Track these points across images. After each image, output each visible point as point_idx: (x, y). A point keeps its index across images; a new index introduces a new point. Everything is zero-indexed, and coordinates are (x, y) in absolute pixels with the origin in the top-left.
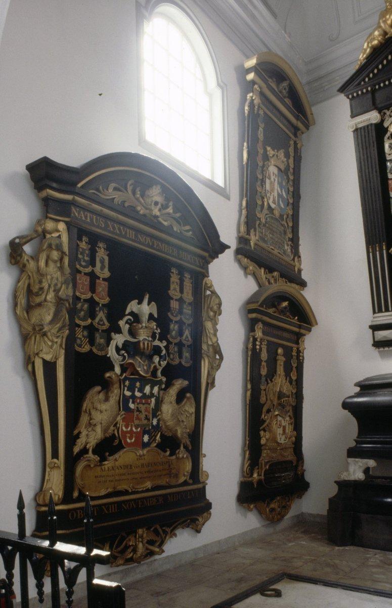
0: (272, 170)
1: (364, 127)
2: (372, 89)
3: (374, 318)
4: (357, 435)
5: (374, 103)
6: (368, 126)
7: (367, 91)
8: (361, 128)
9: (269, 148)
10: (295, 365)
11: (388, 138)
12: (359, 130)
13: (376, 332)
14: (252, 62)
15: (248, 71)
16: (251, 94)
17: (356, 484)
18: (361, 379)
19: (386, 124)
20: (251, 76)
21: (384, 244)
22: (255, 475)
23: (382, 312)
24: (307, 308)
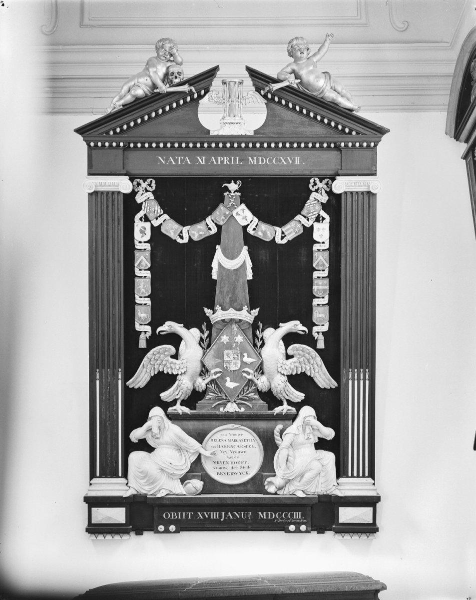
1: (108, 192)
2: (124, 146)
3: (91, 484)
6: (113, 193)
7: (118, 146)
8: (102, 193)
11: (141, 219)
12: (99, 195)
13: (93, 509)
19: (139, 199)
21: (120, 370)
23: (118, 477)
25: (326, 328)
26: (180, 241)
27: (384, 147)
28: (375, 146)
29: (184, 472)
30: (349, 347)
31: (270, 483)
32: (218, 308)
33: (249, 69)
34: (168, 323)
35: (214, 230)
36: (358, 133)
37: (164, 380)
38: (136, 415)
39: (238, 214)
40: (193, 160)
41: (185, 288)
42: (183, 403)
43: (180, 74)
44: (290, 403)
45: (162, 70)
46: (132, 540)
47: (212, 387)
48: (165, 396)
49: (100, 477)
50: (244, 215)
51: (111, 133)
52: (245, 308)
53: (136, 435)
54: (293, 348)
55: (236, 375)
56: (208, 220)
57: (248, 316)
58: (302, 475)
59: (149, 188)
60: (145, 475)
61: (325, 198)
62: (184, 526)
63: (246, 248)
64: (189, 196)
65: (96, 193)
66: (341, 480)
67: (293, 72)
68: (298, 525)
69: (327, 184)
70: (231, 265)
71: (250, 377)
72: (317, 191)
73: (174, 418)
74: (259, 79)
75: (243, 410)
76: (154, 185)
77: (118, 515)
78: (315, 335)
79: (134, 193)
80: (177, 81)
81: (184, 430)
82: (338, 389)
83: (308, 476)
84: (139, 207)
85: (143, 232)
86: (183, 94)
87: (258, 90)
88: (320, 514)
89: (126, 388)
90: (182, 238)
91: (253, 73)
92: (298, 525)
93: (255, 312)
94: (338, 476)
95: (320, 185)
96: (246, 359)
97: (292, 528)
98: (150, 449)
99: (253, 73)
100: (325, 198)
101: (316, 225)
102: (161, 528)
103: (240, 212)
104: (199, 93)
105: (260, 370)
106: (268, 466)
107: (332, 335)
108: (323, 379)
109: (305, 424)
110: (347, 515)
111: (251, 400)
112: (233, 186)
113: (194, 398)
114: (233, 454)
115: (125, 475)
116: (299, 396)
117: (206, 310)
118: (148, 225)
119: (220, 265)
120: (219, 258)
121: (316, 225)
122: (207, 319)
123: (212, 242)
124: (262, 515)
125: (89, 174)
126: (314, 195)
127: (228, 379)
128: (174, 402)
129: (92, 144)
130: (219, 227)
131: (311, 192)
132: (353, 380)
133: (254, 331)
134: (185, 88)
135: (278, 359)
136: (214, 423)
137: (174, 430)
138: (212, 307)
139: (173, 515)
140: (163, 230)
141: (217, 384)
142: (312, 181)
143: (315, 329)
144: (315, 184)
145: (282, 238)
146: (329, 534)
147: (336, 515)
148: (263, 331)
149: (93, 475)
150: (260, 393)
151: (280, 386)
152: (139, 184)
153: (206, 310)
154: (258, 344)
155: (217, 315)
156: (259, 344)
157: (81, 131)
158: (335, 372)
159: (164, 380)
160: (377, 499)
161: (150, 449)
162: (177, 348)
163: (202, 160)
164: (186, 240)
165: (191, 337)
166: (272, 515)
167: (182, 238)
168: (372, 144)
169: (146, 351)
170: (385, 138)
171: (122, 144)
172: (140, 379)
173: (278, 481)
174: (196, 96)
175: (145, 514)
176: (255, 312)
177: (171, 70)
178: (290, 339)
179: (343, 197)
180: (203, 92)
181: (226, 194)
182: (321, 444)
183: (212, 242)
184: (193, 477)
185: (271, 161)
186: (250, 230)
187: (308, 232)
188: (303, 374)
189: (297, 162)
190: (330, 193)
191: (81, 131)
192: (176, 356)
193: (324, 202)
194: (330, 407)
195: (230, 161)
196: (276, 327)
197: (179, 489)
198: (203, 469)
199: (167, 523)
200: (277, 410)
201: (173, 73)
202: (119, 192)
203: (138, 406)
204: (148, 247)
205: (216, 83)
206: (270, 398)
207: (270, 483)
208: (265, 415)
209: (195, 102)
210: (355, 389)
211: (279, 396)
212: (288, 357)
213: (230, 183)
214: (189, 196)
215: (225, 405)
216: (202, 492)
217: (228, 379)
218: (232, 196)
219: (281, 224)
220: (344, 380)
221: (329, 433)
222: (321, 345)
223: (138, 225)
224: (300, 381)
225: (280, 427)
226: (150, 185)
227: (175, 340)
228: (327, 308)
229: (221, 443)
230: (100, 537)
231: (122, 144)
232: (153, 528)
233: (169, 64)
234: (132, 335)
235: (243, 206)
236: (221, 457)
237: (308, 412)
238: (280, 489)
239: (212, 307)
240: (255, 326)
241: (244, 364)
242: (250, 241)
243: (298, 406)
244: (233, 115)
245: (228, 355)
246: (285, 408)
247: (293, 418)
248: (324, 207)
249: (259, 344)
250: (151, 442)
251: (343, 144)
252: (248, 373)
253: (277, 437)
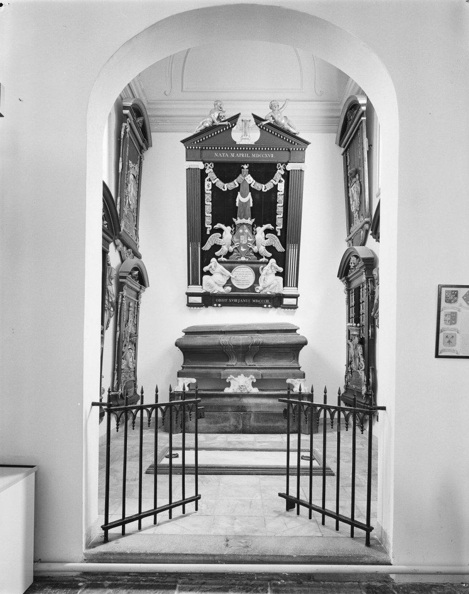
0: (131, 177)
1: (194, 169)
4: (182, 362)
5: (201, 157)
6: (196, 169)
7: (198, 148)
8: (192, 169)
9: (130, 162)
10: (136, 314)
13: (189, 297)
14: (129, 104)
15: (126, 108)
16: (126, 124)
17: (184, 395)
18: (186, 328)
19: (207, 171)
20: (126, 112)
22: (120, 390)
24: (145, 277)
25: (281, 227)
26: (223, 190)
27: (309, 150)
28: (305, 150)
29: (224, 284)
30: (290, 235)
31: (258, 289)
32: (238, 218)
33: (253, 115)
34: (218, 224)
35: (237, 185)
36: (298, 144)
37: (217, 247)
38: (206, 262)
39: (247, 179)
40: (230, 155)
41: (225, 209)
42: (224, 257)
43: (224, 116)
44: (266, 257)
45: (216, 115)
46: (204, 309)
47: (235, 250)
48: (217, 253)
49: (192, 285)
50: (250, 179)
51: (195, 142)
52: (249, 218)
53: (206, 269)
54: (268, 235)
55: (245, 246)
56: (235, 181)
57: (250, 221)
58: (270, 286)
59: (211, 167)
60: (209, 285)
61: (283, 172)
62: (224, 304)
63: (250, 193)
64: (227, 171)
65: (189, 169)
66: (285, 288)
67: (272, 116)
68: (267, 305)
70: (244, 200)
71: (250, 247)
72: (280, 169)
73: (220, 262)
74: (258, 119)
75: (247, 260)
77: (199, 300)
78: (277, 230)
79: (205, 169)
80: (223, 120)
81: (224, 267)
82: (285, 252)
83: (272, 286)
84: (207, 175)
85: (208, 186)
86: (225, 126)
87: (257, 124)
88: (276, 301)
89: (202, 250)
90: (224, 188)
91: (255, 117)
92: (267, 305)
93: (253, 220)
94: (284, 286)
95: (282, 167)
96: (249, 239)
97: (265, 306)
98: (211, 275)
99: (255, 117)
100: (283, 172)
101: (279, 184)
102: (215, 305)
103: (248, 178)
104: (232, 125)
105: (255, 244)
106: (257, 282)
107: (284, 230)
108: (280, 248)
109: (271, 266)
110: (286, 301)
111: (251, 256)
112: (245, 167)
113: (228, 255)
114: (243, 277)
115: (201, 284)
116: (270, 255)
117: (234, 219)
118: (210, 183)
119: (239, 200)
120: (239, 198)
121: (279, 184)
122: (234, 223)
123: (235, 191)
124: (254, 301)
125: (187, 161)
126: (278, 171)
127: (242, 247)
128: (221, 256)
129: (188, 147)
130: (239, 184)
131: (277, 169)
132: (291, 248)
133: (252, 228)
134: (226, 123)
135: (262, 239)
136: (236, 265)
137: (220, 267)
138: (236, 218)
139: (220, 300)
140: (216, 185)
141: (238, 250)
142: (278, 165)
143: (277, 228)
144: (279, 166)
145: (265, 189)
146: (279, 309)
147: (281, 302)
148: (256, 228)
149: (189, 284)
150: (254, 253)
151: (262, 250)
152: (207, 165)
153: (234, 219)
154: (254, 233)
155: (238, 221)
156: (254, 233)
157: (183, 141)
158: (284, 246)
159: (217, 247)
160: (299, 295)
161: (211, 275)
162: (222, 234)
163: (233, 155)
164: (226, 189)
165: (227, 230)
166: (257, 301)
167: (224, 188)
169: (209, 235)
170: (309, 146)
171: (200, 148)
172: (207, 247)
173: (260, 288)
174: (231, 126)
175: (209, 300)
176: (253, 220)
177: (220, 115)
178: (267, 231)
179: (291, 172)
180: (234, 125)
181: (242, 170)
182: (278, 274)
183: (235, 191)
184: (228, 286)
186: (252, 186)
187: (276, 186)
188: (272, 246)
190: (285, 170)
191: (183, 141)
192: (221, 238)
193: (283, 174)
194: (281, 259)
195: (244, 155)
196: (261, 226)
197: (222, 290)
198: (231, 283)
199: (218, 303)
200: (261, 260)
201: (221, 116)
202: (199, 169)
203: (207, 257)
204: (210, 192)
205: (240, 119)
206: (258, 255)
207: (258, 289)
208: (256, 262)
209: (230, 129)
210: (292, 252)
211: (262, 255)
212: (266, 239)
213: (244, 165)
214: (227, 171)
215: (240, 258)
216: (231, 292)
217: (242, 247)
219: (265, 183)
220: (287, 249)
221: (281, 269)
222: (279, 234)
223: (207, 183)
224: (270, 248)
225: (262, 267)
227: (221, 231)
228: (282, 219)
229: (238, 273)
230: (192, 308)
231: (200, 148)
232: (212, 305)
233: (220, 112)
234: (204, 229)
235: (249, 175)
236: (238, 278)
237: (273, 261)
238: (261, 291)
239: (236, 218)
240: (253, 226)
241: (248, 241)
242: (252, 190)
243: (269, 259)
244: (246, 135)
245: (242, 238)
246: (264, 259)
247: (267, 263)
248: (283, 176)
249: (254, 233)
250: (211, 272)
251: (291, 149)
252: (250, 245)
253: (260, 271)
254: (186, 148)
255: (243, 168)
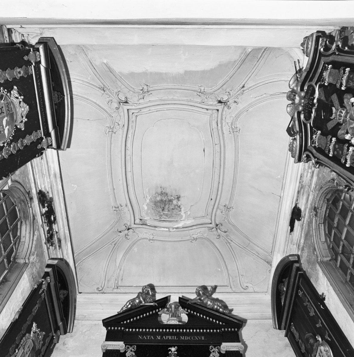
59: (133, 350)
69: (218, 348)
72: (213, 352)
76: (135, 348)
112: (173, 349)
142: (211, 347)
152: (128, 348)
168: (236, 329)
181: (170, 352)
185: (191, 338)
189: (203, 338)
195: (172, 338)
213: (172, 347)
218: (173, 353)
226: (133, 348)
254: (107, 329)
255: (170, 350)
